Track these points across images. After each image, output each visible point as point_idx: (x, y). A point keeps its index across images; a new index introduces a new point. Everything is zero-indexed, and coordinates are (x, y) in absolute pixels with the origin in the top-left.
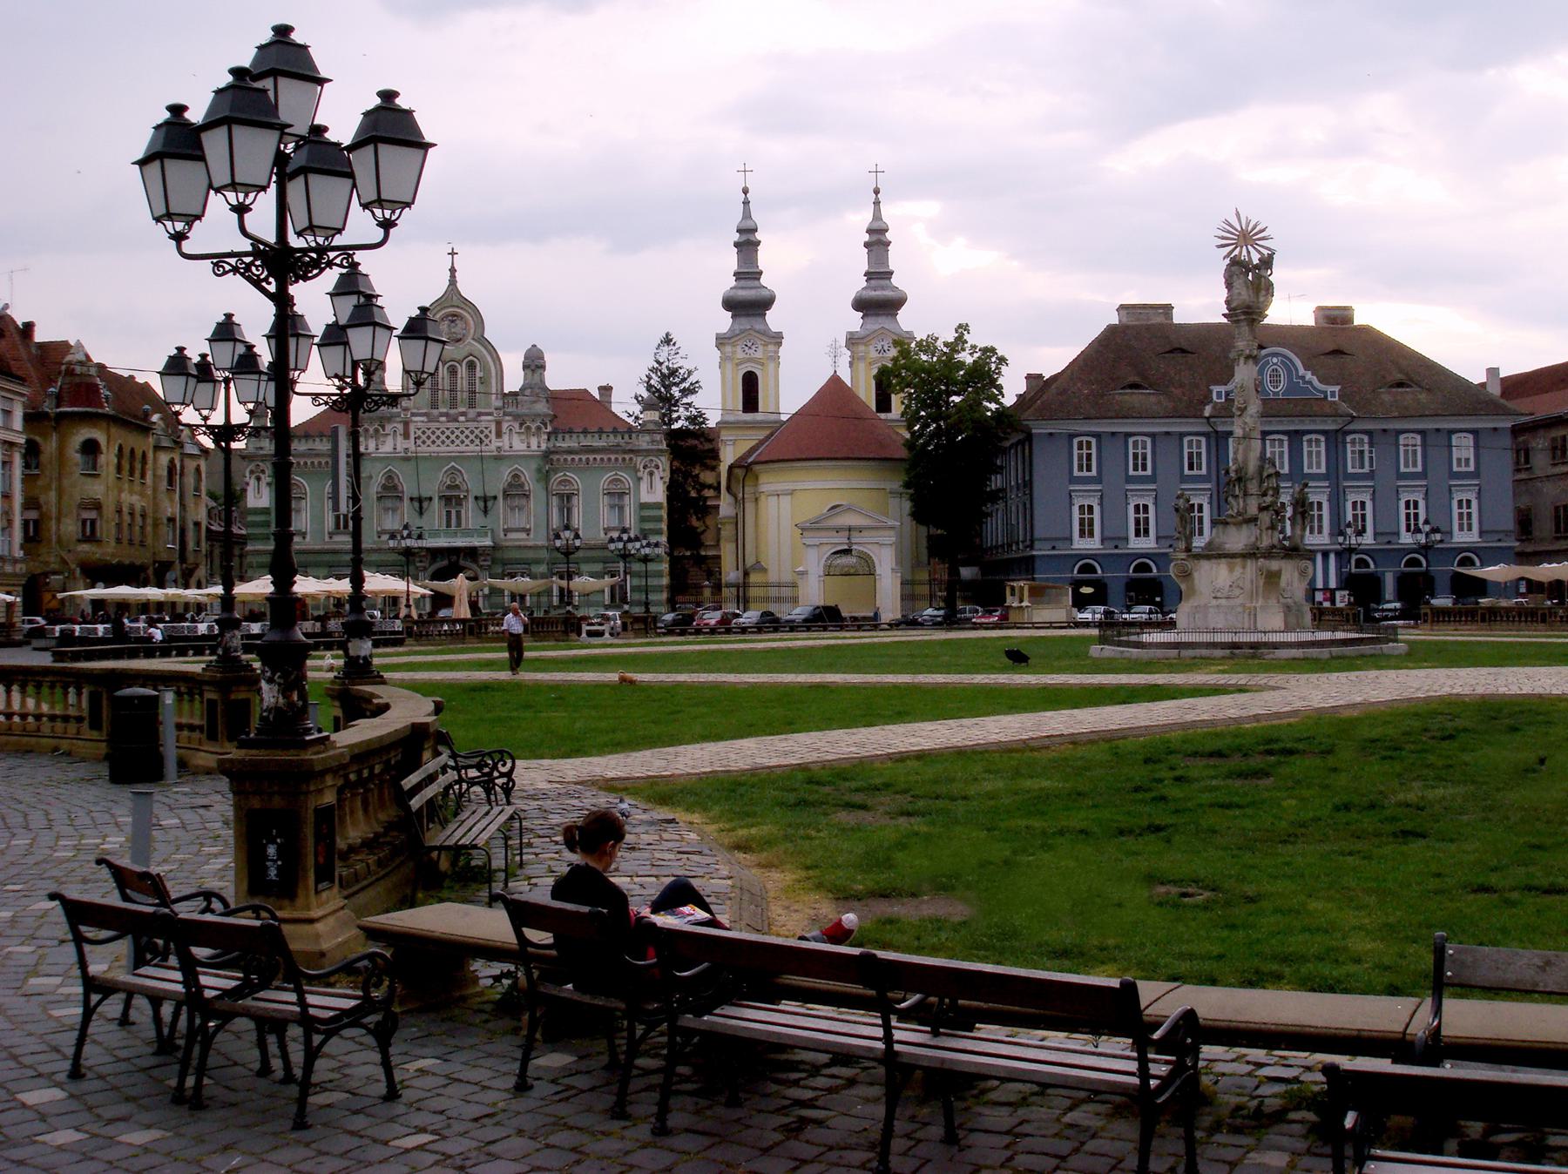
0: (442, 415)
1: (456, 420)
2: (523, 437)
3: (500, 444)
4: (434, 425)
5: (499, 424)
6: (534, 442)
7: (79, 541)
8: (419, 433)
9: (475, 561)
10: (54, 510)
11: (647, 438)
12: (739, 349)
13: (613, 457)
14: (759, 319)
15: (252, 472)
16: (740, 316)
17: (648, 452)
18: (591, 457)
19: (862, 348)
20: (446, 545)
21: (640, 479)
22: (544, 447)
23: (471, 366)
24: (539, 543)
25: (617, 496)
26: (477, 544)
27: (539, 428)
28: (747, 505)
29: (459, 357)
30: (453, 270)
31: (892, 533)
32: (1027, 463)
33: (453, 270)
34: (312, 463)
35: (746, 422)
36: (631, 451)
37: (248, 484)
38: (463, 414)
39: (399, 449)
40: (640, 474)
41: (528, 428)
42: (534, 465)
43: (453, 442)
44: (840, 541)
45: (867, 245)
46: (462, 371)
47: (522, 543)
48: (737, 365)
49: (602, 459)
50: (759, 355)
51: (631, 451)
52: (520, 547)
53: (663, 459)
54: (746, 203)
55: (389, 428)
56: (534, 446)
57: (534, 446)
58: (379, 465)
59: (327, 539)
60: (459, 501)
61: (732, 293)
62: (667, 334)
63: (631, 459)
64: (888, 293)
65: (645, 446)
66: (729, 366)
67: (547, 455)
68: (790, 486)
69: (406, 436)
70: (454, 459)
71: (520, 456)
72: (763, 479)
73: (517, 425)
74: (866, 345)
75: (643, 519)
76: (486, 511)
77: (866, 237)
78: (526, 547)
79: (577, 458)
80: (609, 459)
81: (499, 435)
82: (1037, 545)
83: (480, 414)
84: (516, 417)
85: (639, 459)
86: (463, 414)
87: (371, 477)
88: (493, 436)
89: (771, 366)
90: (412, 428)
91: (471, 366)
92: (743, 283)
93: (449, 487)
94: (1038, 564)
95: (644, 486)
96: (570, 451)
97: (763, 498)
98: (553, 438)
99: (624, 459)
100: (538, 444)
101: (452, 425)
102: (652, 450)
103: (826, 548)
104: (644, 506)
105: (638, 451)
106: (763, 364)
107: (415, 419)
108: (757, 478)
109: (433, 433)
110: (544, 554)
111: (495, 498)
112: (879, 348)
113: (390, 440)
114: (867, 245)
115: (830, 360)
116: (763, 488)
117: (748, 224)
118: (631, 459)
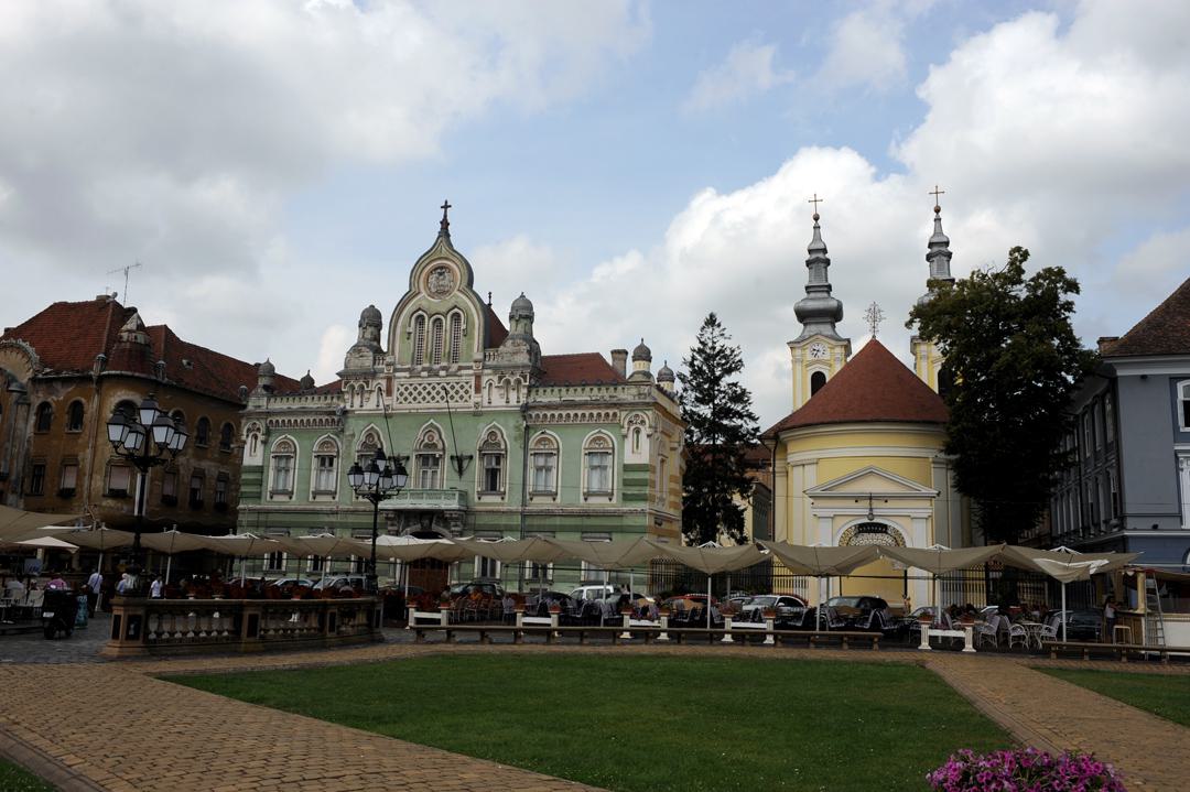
0: (424, 369)
1: (437, 376)
2: (502, 391)
3: (479, 400)
4: (415, 381)
5: (478, 377)
6: (513, 396)
7: (104, 496)
8: (402, 389)
9: (447, 526)
10: (88, 466)
11: (634, 391)
13: (595, 412)
15: (249, 430)
16: (810, 323)
17: (632, 406)
18: (572, 413)
20: (411, 507)
21: (625, 436)
22: (523, 400)
23: (456, 317)
24: (513, 508)
25: (599, 453)
26: (443, 507)
27: (519, 382)
29: (444, 310)
30: (445, 224)
31: (927, 504)
32: (1109, 421)
33: (445, 224)
34: (302, 421)
36: (615, 405)
37: (245, 442)
38: (443, 368)
39: (381, 407)
40: (624, 431)
41: (508, 382)
42: (512, 422)
43: (433, 398)
44: (860, 514)
46: (447, 323)
47: (497, 508)
48: (807, 366)
49: (584, 415)
50: (827, 357)
51: (615, 405)
52: (492, 512)
53: (649, 413)
55: (373, 384)
56: (513, 401)
57: (513, 401)
58: (362, 423)
59: (311, 499)
60: (436, 461)
62: (712, 316)
63: (615, 414)
65: (630, 399)
66: (799, 367)
67: (526, 408)
68: (813, 455)
69: (389, 393)
70: (433, 415)
71: (500, 412)
72: (791, 448)
73: (496, 378)
75: (626, 483)
76: (461, 472)
78: (498, 512)
79: (556, 413)
80: (591, 415)
81: (478, 389)
82: (1130, 523)
83: (460, 368)
84: (496, 369)
85: (624, 414)
86: (443, 368)
87: (353, 435)
88: (472, 391)
90: (396, 384)
91: (456, 317)
93: (427, 446)
94: (1131, 544)
95: (628, 443)
96: (548, 407)
98: (533, 393)
99: (607, 415)
100: (517, 398)
101: (434, 380)
102: (637, 404)
103: (840, 522)
104: (627, 468)
105: (621, 405)
106: (830, 366)
107: (397, 374)
109: (415, 389)
110: (517, 520)
111: (471, 457)
113: (374, 396)
115: (868, 325)
118: (615, 414)
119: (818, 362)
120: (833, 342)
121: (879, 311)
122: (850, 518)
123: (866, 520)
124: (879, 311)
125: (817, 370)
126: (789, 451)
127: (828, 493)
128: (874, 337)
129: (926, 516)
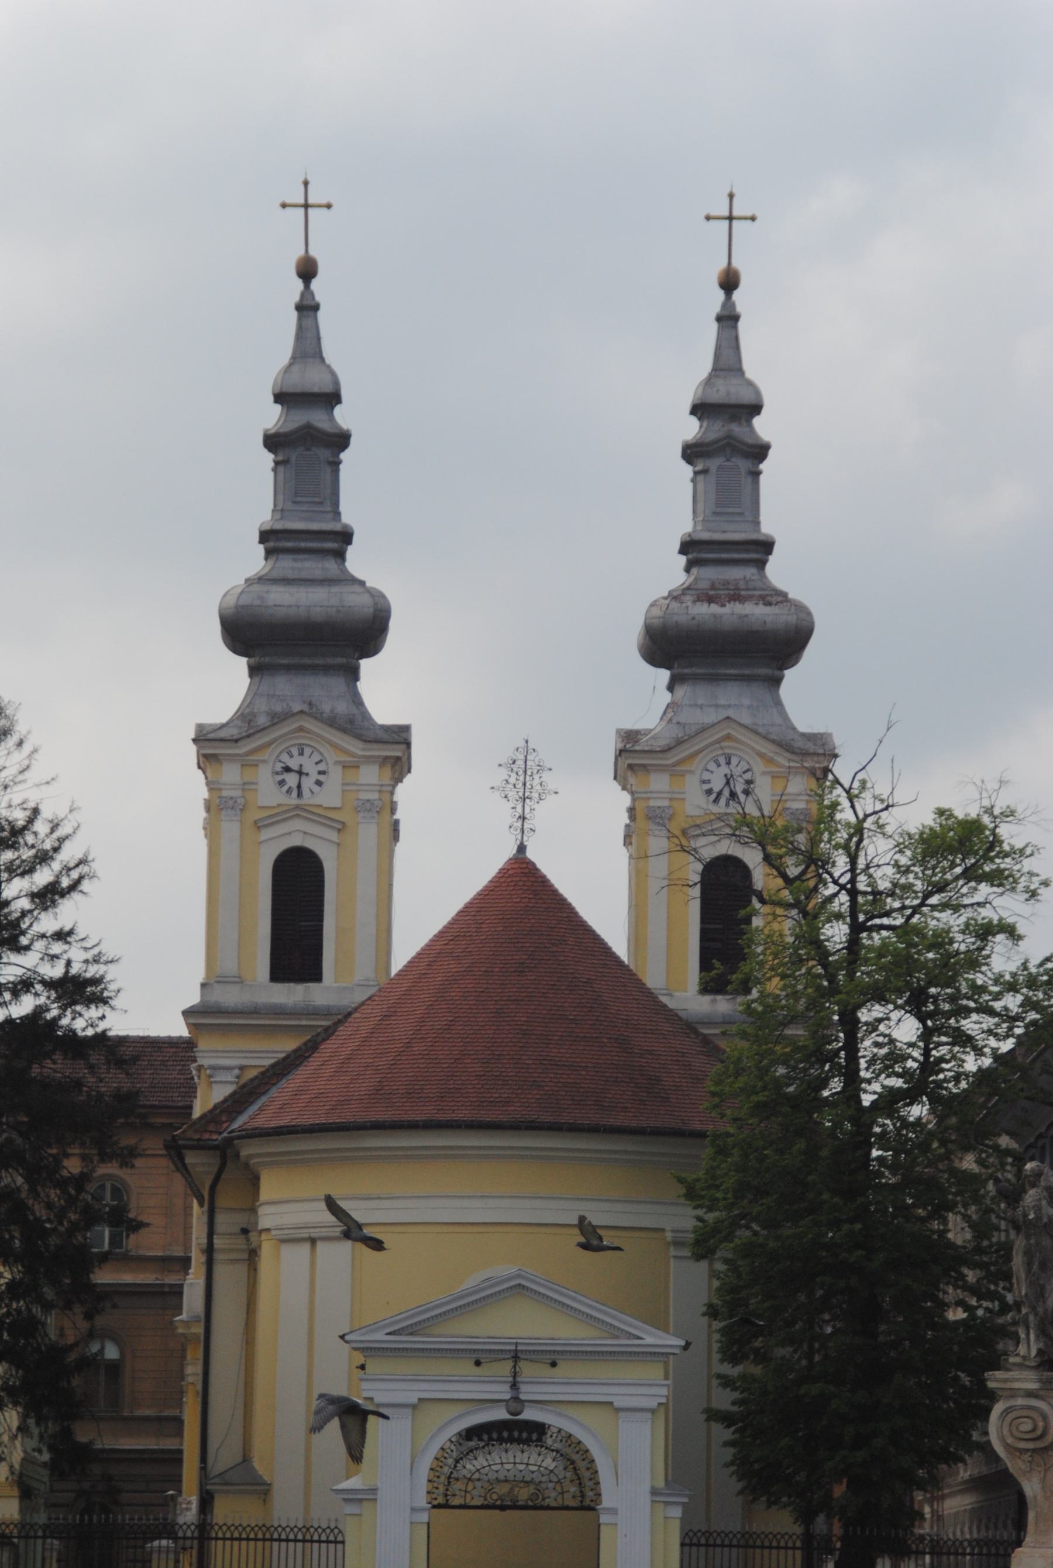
12: (265, 777)
14: (337, 684)
19: (659, 782)
28: (221, 1271)
31: (655, 1372)
35: (279, 1011)
45: (691, 453)
48: (258, 826)
50: (329, 796)
54: (307, 308)
61: (245, 600)
64: (754, 612)
66: (231, 829)
72: (270, 1186)
74: (675, 771)
77: (691, 429)
89: (367, 834)
92: (287, 565)
97: (267, 1249)
106: (341, 828)
108: (255, 1181)
112: (717, 784)
114: (691, 453)
115: (504, 812)
116: (268, 1217)
117: (313, 380)
119: (299, 812)
120: (356, 747)
121: (541, 768)
122: (455, 1410)
123: (501, 1414)
124: (541, 768)
125: (296, 841)
126: (264, 1195)
127: (405, 1341)
128: (522, 848)
129: (653, 1403)
